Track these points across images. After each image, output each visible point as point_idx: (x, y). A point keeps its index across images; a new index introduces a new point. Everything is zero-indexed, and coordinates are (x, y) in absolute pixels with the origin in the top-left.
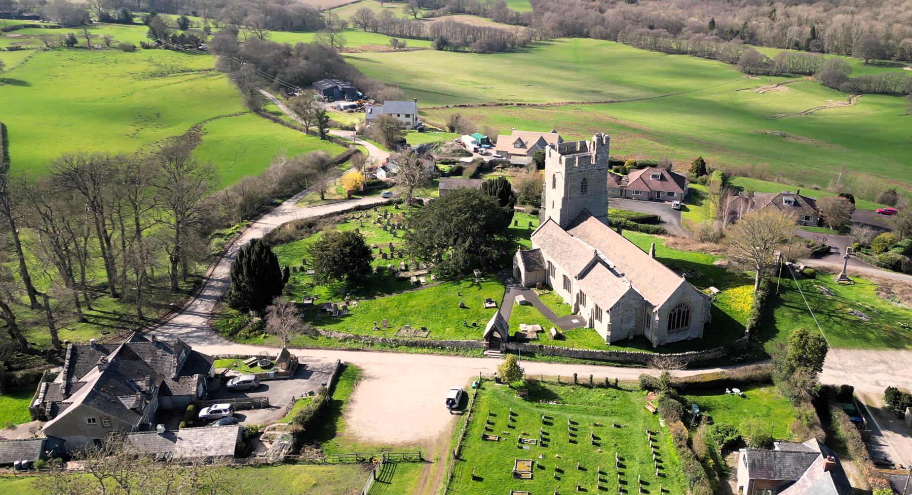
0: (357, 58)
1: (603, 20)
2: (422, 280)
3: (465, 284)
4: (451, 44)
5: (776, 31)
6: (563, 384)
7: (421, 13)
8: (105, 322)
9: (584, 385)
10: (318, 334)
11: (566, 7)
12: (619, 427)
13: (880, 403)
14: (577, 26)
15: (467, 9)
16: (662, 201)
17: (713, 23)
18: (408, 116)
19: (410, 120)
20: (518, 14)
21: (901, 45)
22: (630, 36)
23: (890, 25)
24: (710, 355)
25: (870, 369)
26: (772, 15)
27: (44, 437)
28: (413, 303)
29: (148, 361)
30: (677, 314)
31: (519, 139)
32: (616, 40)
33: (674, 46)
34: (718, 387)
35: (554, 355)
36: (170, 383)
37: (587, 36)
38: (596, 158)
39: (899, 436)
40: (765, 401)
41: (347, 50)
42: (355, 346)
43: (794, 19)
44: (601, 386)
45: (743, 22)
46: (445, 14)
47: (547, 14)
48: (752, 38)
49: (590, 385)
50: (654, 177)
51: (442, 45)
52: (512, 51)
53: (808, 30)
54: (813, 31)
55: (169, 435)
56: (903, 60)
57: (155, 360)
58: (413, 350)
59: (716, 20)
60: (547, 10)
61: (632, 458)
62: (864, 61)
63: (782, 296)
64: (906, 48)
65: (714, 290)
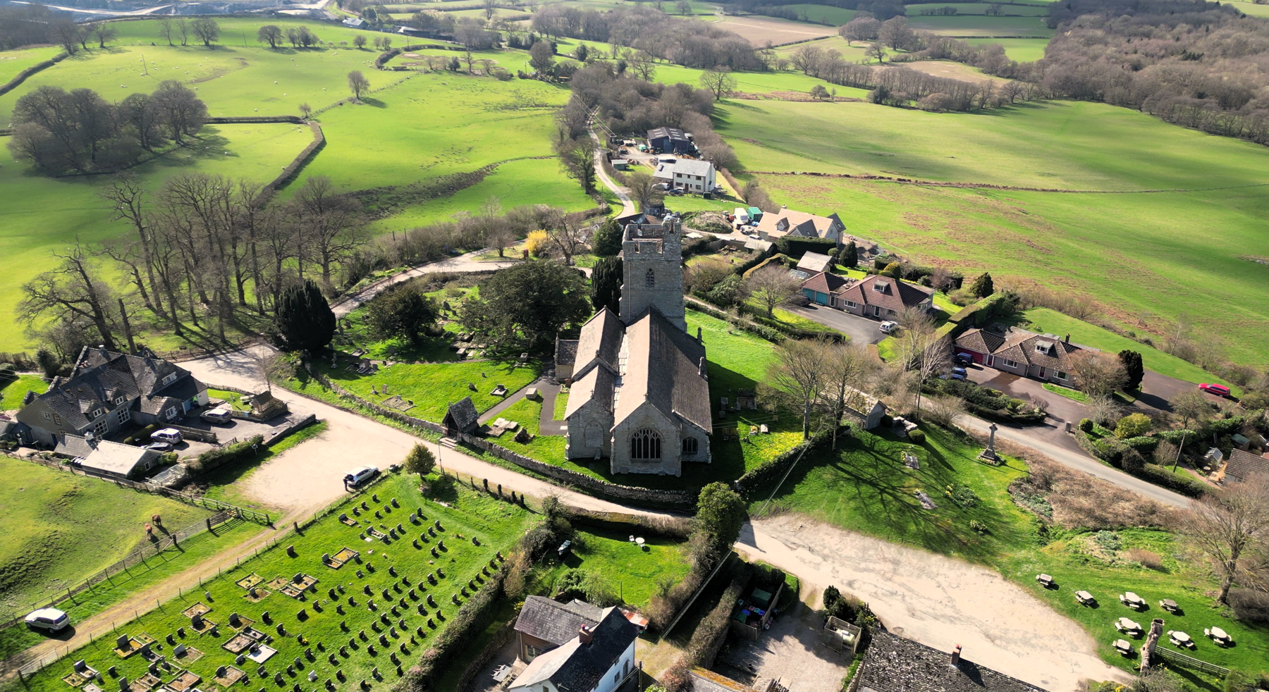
0: (743, 106)
1: (1130, 79)
2: (471, 354)
3: (503, 365)
4: (892, 97)
6: (475, 488)
7: (890, 53)
8: (193, 339)
9: (493, 495)
10: (329, 387)
12: (478, 544)
13: (818, 605)
14: (1090, 85)
15: (955, 53)
16: (879, 320)
18: (699, 178)
19: (700, 183)
20: (1015, 64)
24: (666, 497)
25: (863, 565)
27: (15, 420)
28: (436, 375)
29: (136, 375)
30: (644, 443)
31: (785, 221)
34: (621, 530)
35: (503, 457)
36: (144, 399)
37: (1100, 99)
39: (801, 647)
40: (661, 563)
41: (736, 95)
42: (347, 406)
44: (506, 499)
46: (923, 59)
47: (1054, 66)
49: (498, 495)
50: (877, 287)
51: (881, 97)
52: (979, 111)
55: (93, 444)
57: (141, 377)
58: (388, 421)
60: (1056, 61)
61: (453, 577)
63: (844, 454)
65: (764, 428)
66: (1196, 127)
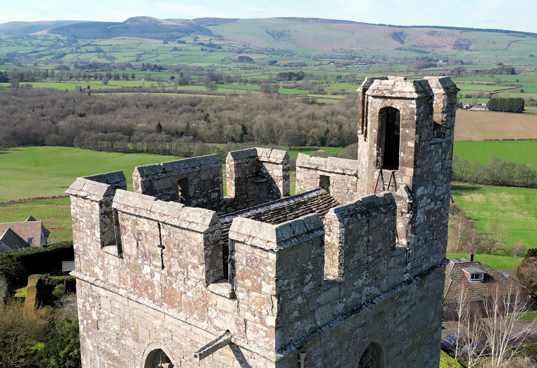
5: (214, 130)
11: (18, 120)
17: (159, 128)
21: (311, 134)
22: (86, 142)
23: (298, 121)
26: (206, 118)
32: (72, 146)
33: (130, 146)
38: (413, 208)
43: (226, 120)
45: (186, 125)
48: (196, 137)
53: (239, 127)
54: (244, 128)
56: (315, 145)
59: (162, 124)
62: (289, 148)
64: (314, 136)
66: (116, 151)
